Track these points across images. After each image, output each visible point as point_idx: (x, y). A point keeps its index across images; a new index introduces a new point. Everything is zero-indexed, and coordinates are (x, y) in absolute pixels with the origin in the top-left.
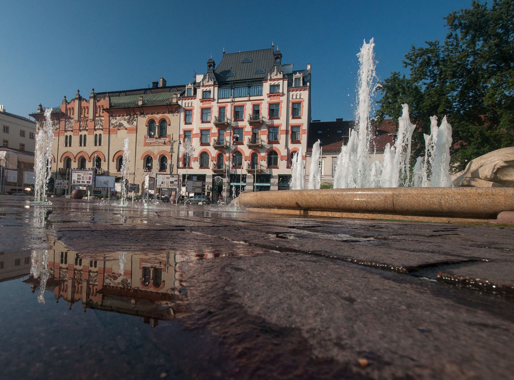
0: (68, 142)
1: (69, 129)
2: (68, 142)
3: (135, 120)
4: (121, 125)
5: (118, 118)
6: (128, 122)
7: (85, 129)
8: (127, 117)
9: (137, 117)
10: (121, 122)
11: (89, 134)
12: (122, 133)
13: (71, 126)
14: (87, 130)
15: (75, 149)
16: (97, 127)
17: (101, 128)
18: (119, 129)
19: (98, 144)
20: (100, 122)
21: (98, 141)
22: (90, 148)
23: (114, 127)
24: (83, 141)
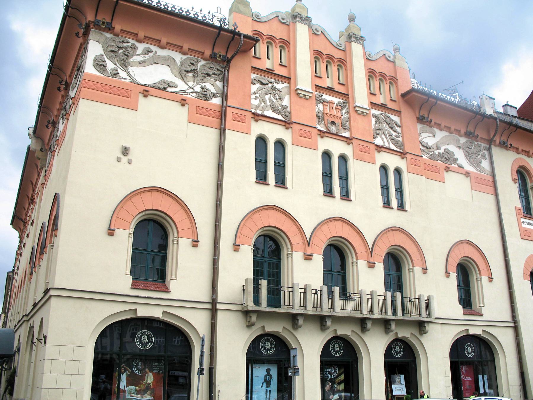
0: (270, 165)
1: (269, 113)
2: (270, 165)
3: (484, 157)
4: (448, 158)
5: (440, 134)
6: (468, 155)
7: (336, 136)
8: (463, 140)
9: (489, 150)
10: (452, 148)
11: (356, 158)
12: (456, 185)
13: (277, 103)
14: (348, 140)
15: (304, 202)
16: (378, 141)
17: (393, 147)
18: (447, 169)
19: (394, 203)
20: (385, 125)
21: (392, 191)
22: (367, 214)
23: (432, 158)
24: (335, 178)
